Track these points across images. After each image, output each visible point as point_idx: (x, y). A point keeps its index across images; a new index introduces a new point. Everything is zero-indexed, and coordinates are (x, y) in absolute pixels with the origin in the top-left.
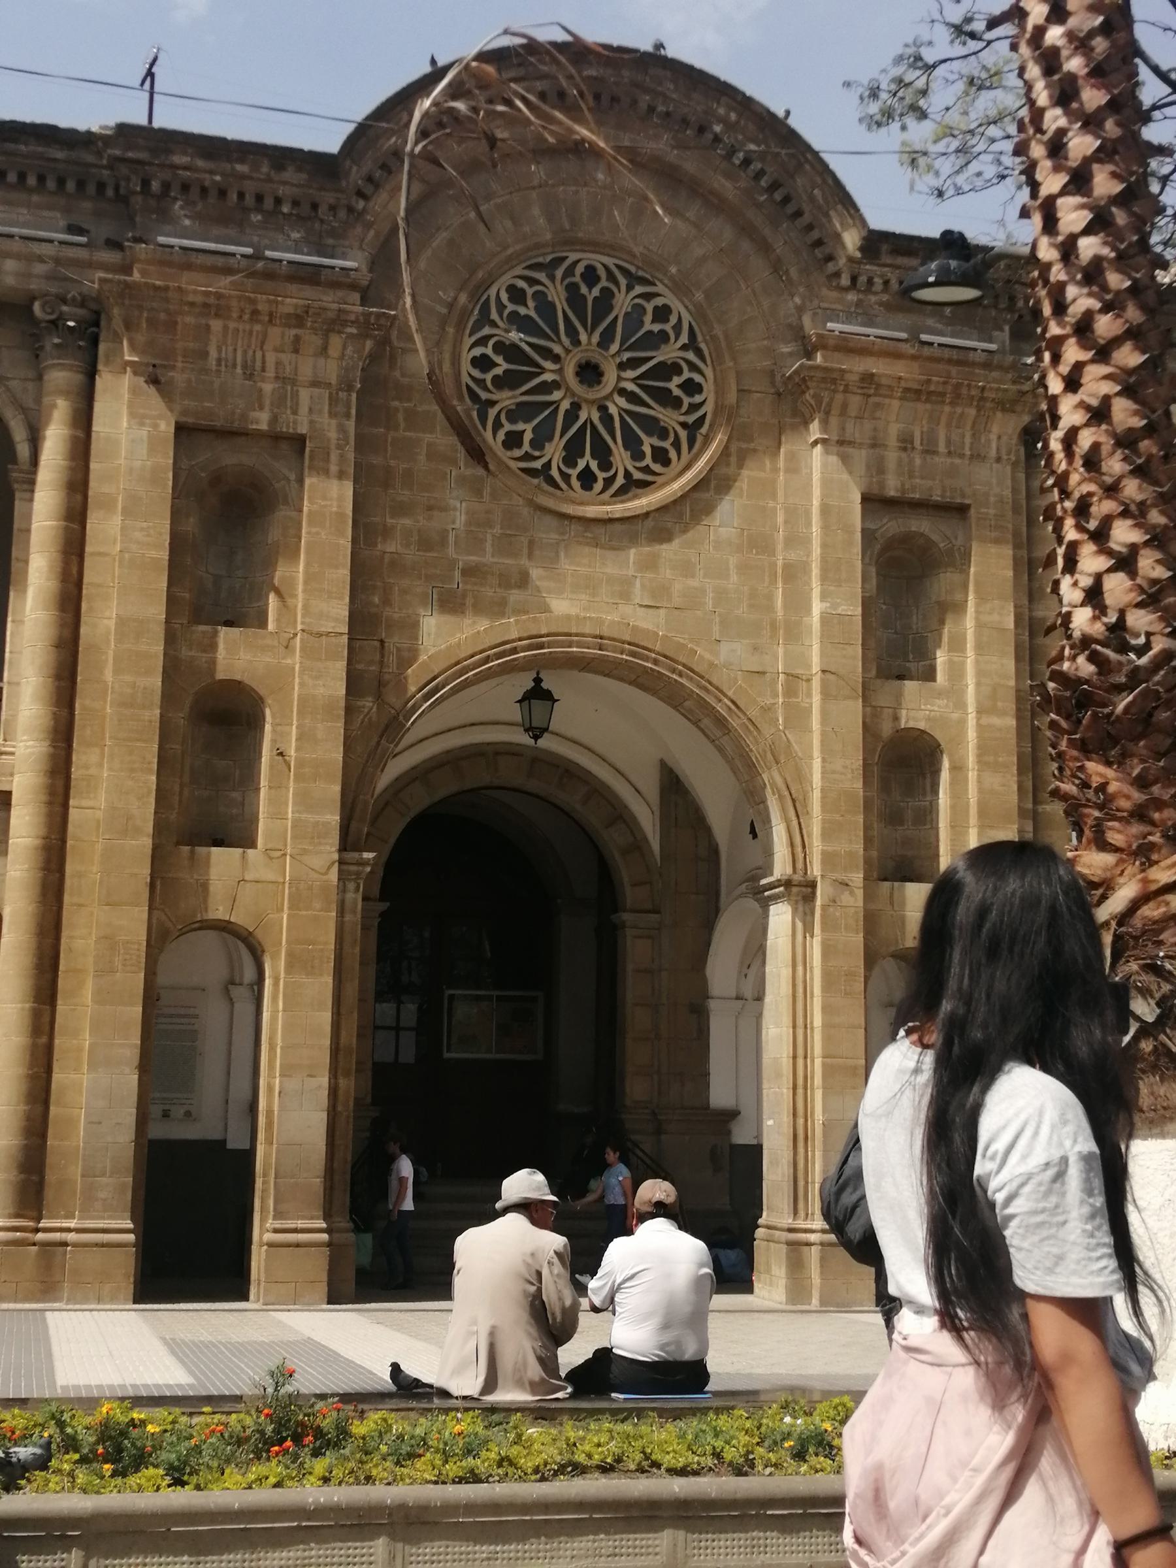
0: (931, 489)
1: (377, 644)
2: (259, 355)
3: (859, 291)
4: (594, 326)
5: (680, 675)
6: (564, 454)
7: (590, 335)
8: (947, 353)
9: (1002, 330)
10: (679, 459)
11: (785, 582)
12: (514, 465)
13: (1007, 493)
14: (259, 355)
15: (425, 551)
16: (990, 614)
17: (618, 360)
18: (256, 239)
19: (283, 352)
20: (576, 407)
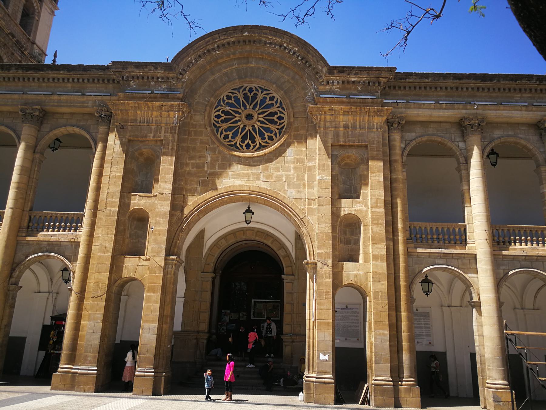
0: (355, 140)
1: (183, 196)
2: (151, 118)
4: (251, 104)
5: (274, 201)
6: (241, 139)
7: (250, 106)
9: (378, 92)
11: (308, 172)
12: (225, 143)
13: (381, 140)
14: (151, 118)
15: (198, 169)
16: (375, 177)
17: (258, 112)
18: (153, 89)
19: (157, 117)
20: (245, 126)
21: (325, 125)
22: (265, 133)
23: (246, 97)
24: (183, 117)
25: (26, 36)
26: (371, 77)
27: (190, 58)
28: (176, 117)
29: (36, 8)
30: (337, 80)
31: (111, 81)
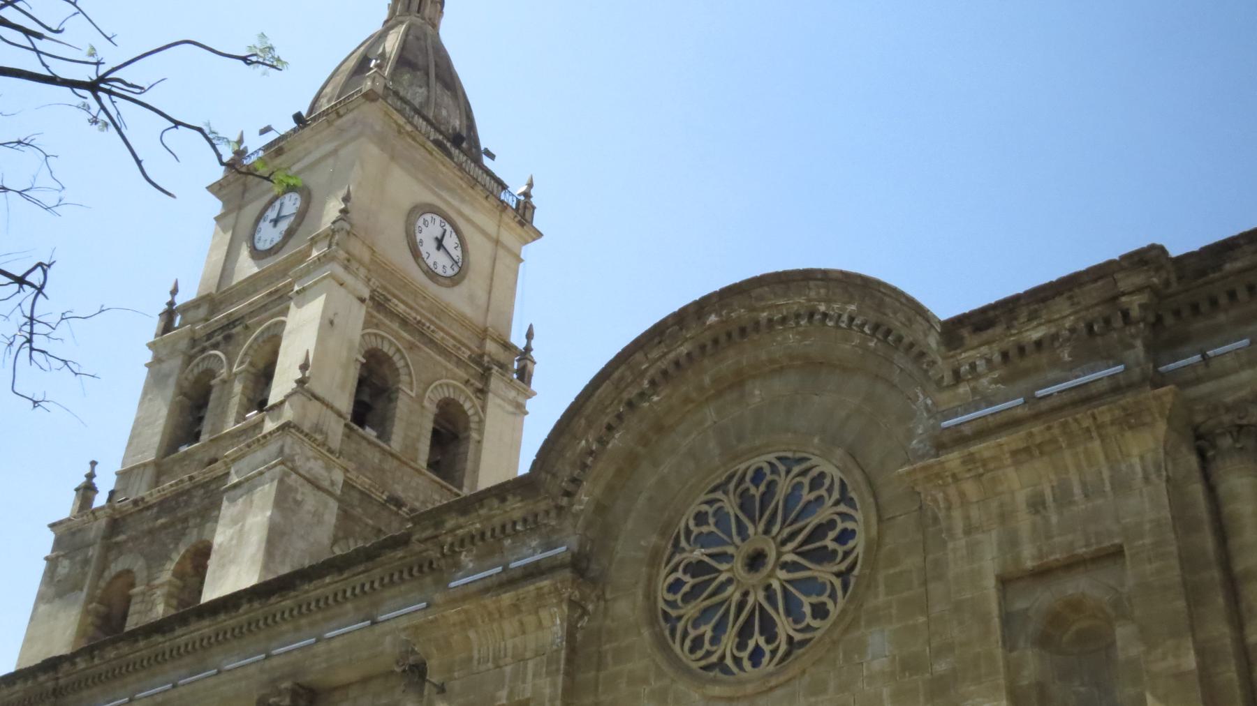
2: (502, 644)
3: (968, 381)
6: (737, 640)
7: (756, 527)
8: (1066, 398)
10: (835, 606)
13: (1166, 514)
17: (779, 538)
21: (967, 518)
22: (803, 598)
23: (745, 503)
24: (581, 617)
25: (450, 490)
26: (1087, 309)
27: (583, 442)
28: (558, 622)
29: (470, 412)
30: (982, 357)
31: (426, 569)
